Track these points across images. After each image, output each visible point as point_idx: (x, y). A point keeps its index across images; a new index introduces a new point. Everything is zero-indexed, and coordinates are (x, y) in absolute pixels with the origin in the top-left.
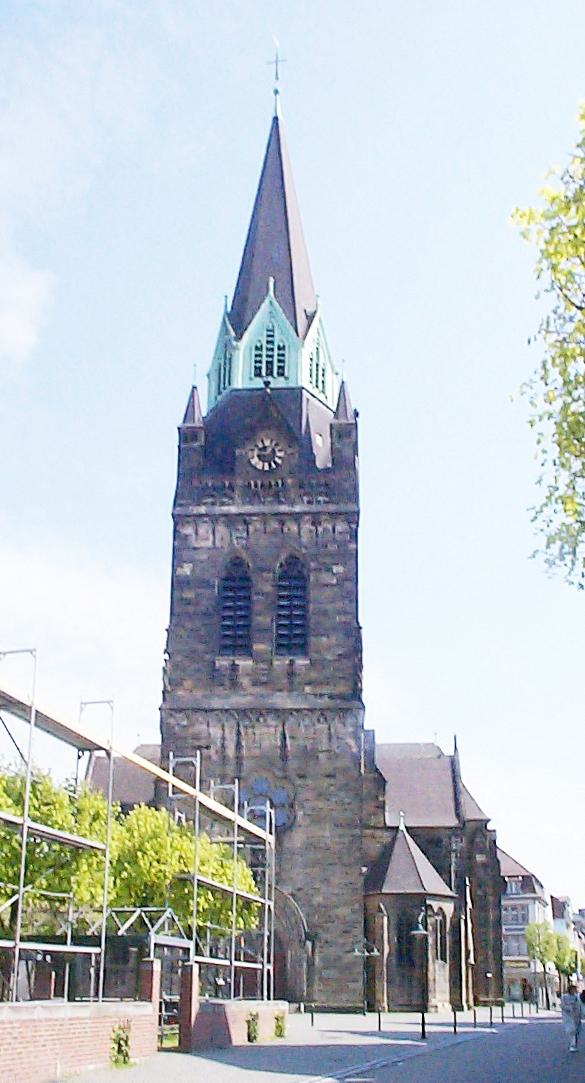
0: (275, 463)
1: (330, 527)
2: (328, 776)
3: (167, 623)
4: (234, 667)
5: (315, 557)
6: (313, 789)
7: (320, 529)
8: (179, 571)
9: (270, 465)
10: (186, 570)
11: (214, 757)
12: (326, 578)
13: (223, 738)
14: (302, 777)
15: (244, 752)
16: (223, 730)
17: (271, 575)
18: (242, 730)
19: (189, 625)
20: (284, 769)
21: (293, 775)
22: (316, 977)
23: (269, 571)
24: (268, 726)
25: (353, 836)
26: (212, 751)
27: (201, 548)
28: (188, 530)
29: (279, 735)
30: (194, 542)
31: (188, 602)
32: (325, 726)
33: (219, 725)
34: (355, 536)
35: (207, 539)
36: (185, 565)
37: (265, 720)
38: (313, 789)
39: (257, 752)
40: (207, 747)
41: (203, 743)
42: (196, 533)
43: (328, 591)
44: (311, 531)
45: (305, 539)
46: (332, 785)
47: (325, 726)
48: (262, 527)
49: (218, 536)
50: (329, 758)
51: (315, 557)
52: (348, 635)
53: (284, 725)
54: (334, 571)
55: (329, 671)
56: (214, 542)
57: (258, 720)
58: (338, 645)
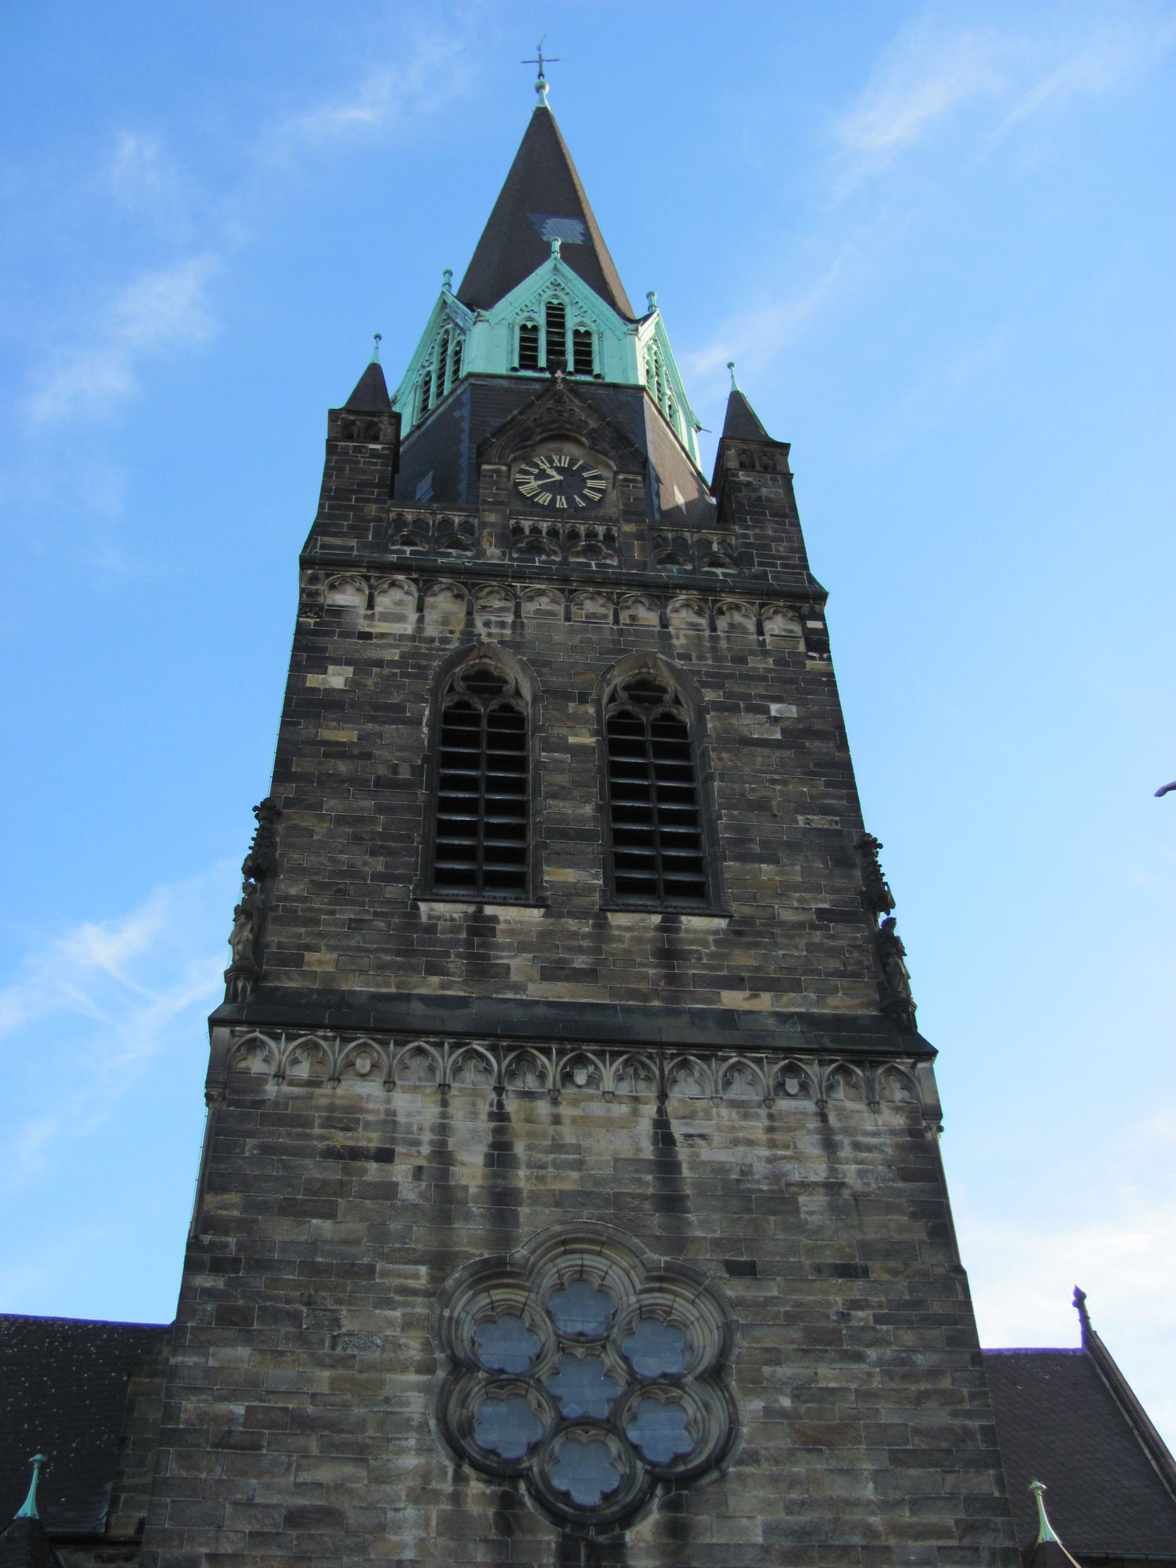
0: (585, 498)
1: (751, 625)
2: (847, 1271)
3: (262, 789)
4: (481, 927)
5: (717, 680)
6: (791, 1319)
7: (722, 623)
8: (313, 680)
9: (570, 500)
10: (336, 679)
12: (749, 724)
13: (443, 1129)
14: (744, 1270)
15: (522, 1178)
16: (444, 1103)
17: (591, 710)
18: (512, 1105)
19: (332, 805)
20: (678, 1243)
21: (708, 1261)
23: (583, 699)
24: (610, 1097)
25: (970, 1499)
26: (400, 1172)
27: (382, 636)
28: (348, 598)
29: (645, 1126)
30: (361, 621)
31: (339, 751)
32: (809, 1105)
33: (430, 1087)
34: (819, 643)
35: (402, 618)
36: (331, 669)
37: (592, 1080)
38: (791, 1319)
39: (570, 1181)
40: (385, 1156)
41: (371, 1139)
42: (371, 605)
43: (760, 757)
44: (694, 626)
45: (679, 643)
46: (855, 1305)
47: (809, 1105)
48: (560, 609)
49: (431, 616)
50: (834, 1208)
51: (717, 680)
52: (842, 862)
53: (663, 1096)
54: (773, 713)
55: (794, 951)
56: (420, 628)
57: (567, 1078)
58: (817, 888)
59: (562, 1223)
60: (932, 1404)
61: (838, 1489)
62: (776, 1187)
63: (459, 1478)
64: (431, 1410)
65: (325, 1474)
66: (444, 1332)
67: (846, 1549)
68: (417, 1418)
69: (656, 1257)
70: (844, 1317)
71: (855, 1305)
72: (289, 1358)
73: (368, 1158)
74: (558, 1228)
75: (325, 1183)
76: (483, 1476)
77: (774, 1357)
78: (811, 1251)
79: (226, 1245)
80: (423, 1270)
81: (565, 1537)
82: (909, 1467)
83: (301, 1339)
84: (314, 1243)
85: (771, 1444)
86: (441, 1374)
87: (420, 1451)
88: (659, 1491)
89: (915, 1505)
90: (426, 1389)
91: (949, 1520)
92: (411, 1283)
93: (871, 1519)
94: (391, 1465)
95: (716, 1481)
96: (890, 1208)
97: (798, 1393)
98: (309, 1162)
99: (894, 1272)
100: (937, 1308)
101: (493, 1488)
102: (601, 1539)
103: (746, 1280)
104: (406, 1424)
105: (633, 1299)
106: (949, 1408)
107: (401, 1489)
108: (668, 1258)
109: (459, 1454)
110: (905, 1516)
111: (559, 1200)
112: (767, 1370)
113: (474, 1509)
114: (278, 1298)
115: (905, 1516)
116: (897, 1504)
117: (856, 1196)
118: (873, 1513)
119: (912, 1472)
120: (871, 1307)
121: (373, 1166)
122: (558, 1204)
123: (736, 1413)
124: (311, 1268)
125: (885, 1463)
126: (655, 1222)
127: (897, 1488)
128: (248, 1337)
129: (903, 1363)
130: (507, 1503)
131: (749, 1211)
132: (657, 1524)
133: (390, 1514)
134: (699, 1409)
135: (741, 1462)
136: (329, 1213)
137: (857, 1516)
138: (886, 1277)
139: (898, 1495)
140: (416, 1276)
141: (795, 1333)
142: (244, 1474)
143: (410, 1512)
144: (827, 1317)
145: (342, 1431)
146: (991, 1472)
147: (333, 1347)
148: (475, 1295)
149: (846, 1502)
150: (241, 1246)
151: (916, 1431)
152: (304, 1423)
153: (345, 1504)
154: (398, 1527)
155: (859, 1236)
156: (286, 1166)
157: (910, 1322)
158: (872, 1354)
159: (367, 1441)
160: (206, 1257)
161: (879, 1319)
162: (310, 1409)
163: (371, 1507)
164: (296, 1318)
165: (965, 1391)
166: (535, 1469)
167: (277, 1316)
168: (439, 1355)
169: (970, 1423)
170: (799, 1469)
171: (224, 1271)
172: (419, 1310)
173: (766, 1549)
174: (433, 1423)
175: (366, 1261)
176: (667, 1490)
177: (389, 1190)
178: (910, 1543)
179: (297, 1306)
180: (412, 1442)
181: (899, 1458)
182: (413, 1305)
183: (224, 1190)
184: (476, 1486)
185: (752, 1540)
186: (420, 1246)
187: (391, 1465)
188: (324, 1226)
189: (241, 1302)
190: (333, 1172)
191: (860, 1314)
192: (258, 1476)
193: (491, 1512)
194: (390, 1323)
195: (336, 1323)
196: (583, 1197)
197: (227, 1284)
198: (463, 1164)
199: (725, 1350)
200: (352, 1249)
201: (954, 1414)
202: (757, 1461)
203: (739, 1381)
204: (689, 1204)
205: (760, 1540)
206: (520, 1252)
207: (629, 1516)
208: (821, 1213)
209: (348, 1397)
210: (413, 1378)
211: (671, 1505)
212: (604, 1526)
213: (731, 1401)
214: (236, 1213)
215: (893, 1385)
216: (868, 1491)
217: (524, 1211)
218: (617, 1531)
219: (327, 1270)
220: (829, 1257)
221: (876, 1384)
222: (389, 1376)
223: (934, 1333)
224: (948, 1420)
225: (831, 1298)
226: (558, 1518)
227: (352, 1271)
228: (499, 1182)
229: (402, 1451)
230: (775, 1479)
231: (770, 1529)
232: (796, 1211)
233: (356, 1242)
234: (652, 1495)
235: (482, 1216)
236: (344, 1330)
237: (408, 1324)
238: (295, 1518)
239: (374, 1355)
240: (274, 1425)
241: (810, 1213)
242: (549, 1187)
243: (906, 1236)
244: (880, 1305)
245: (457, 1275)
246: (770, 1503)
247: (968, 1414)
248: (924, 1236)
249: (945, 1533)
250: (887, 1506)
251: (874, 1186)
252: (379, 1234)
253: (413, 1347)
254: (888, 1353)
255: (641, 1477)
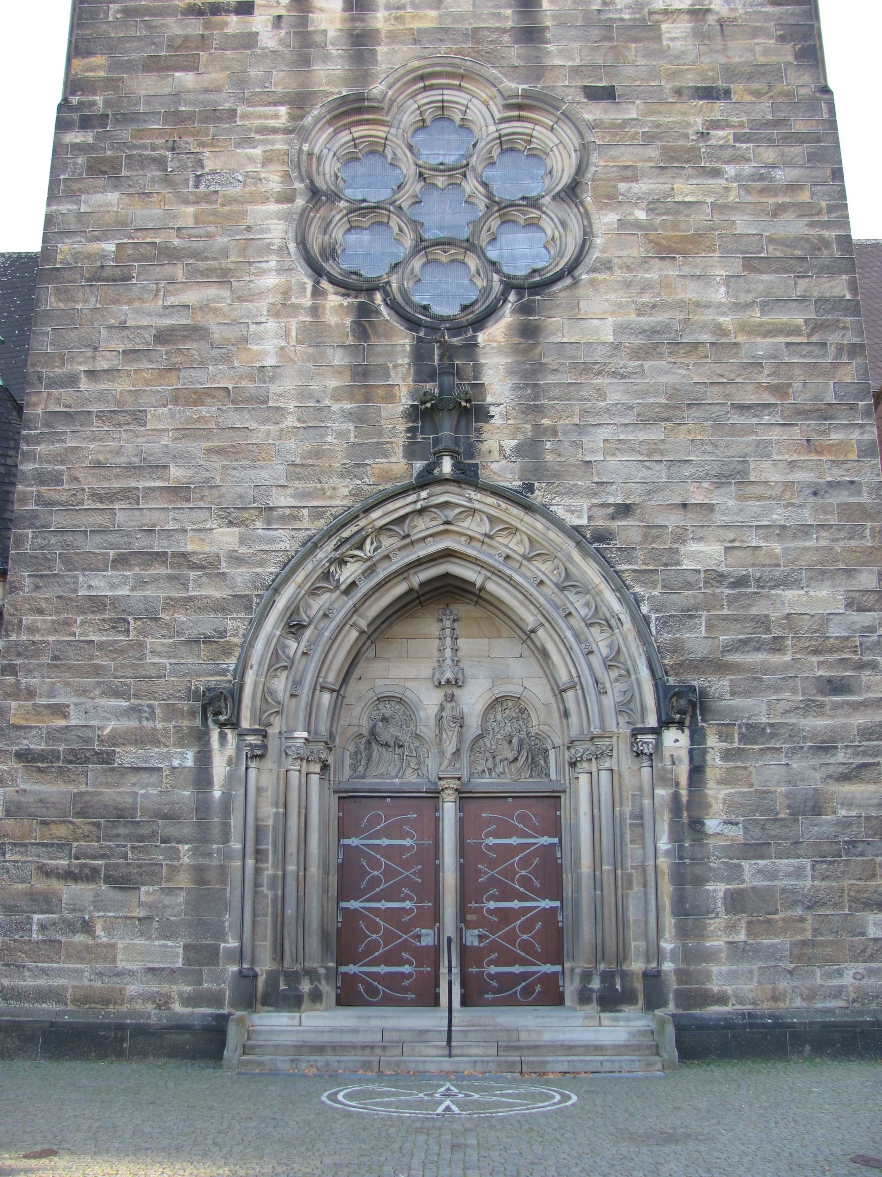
2: (708, 93)
6: (649, 139)
11: (269, 39)
20: (537, 71)
22: (718, 889)
25: (821, 302)
38: (649, 139)
46: (716, 125)
50: (700, 35)
59: (421, 58)
60: (789, 216)
61: (691, 292)
62: (638, 16)
63: (317, 292)
64: (291, 235)
65: (191, 296)
66: (303, 165)
67: (696, 345)
68: (277, 243)
69: (514, 86)
70: (703, 135)
71: (716, 125)
72: (155, 198)
73: (227, 12)
74: (416, 64)
75: (186, 38)
76: (343, 291)
77: (631, 174)
78: (673, 75)
79: (94, 103)
80: (283, 110)
81: (419, 340)
82: (762, 273)
83: (167, 181)
84: (178, 94)
85: (624, 253)
86: (300, 202)
87: (280, 271)
88: (512, 297)
89: (765, 306)
90: (285, 217)
91: (798, 320)
92: (272, 123)
93: (721, 319)
94: (253, 286)
95: (568, 287)
96: (756, 32)
97: (653, 206)
98: (170, 21)
99: (757, 94)
100: (799, 126)
101: (350, 300)
102: (455, 341)
103: (604, 104)
104: (267, 249)
105: (492, 128)
106: (806, 220)
107: (262, 305)
108: (526, 87)
109: (317, 271)
110: (756, 316)
111: (416, 37)
112: (623, 186)
113: (331, 319)
114: (144, 147)
115: (756, 316)
116: (750, 305)
117: (721, 23)
118: (723, 314)
119: (765, 277)
120: (733, 127)
121: (233, 19)
122: (415, 42)
123: (590, 225)
124: (176, 117)
125: (737, 267)
126: (514, 54)
127: (748, 291)
128: (116, 182)
129: (762, 178)
130: (364, 312)
131: (611, 39)
132: (509, 327)
133: (253, 328)
134: (556, 227)
135: (594, 270)
136: (192, 67)
137: (708, 316)
138: (748, 98)
139: (750, 298)
140: (276, 116)
141: (653, 152)
142: (116, 302)
143: (272, 325)
144: (686, 136)
145: (206, 258)
146: (845, 277)
147: (197, 187)
148: (336, 133)
149: (697, 304)
150: (108, 104)
151: (771, 240)
152: (170, 254)
153: (211, 322)
154: (260, 338)
155: (722, 60)
156: (149, 27)
157: (769, 140)
158: (730, 170)
159: (232, 266)
160: (76, 116)
161: (738, 138)
162: (176, 242)
163: (235, 322)
164: (161, 162)
165: (824, 204)
166: (394, 286)
167: (143, 163)
168: (298, 185)
169: (826, 234)
170: (653, 276)
171: (93, 127)
172: (279, 146)
173: (616, 347)
174: (292, 246)
175: (227, 106)
176: (520, 296)
177: (249, 40)
178: (759, 340)
179: (162, 152)
180: (273, 264)
181: (752, 264)
182: (273, 143)
183: (89, 54)
184: (334, 299)
185: (603, 339)
186: (279, 89)
187: (253, 286)
188: (187, 79)
189: (109, 153)
190: (195, 27)
191: (720, 133)
192: (130, 302)
193: (348, 321)
194: (251, 159)
195: (200, 163)
196: (442, 33)
197: (96, 138)
198: (322, 10)
199: (581, 170)
200: (213, 97)
201: (811, 225)
202: (610, 269)
203: (595, 197)
204: (548, 35)
205: (611, 339)
206: (377, 89)
207: (480, 322)
208: (684, 39)
209: (211, 229)
210: (273, 207)
211: (525, 309)
212: (457, 329)
213: (586, 215)
214: (102, 74)
215: (749, 199)
216: (720, 295)
217: (382, 50)
218: (470, 333)
219: (191, 116)
220: (690, 80)
221: (732, 198)
222: (249, 208)
223: (797, 151)
224: (806, 231)
225: (691, 119)
226: (412, 324)
227: (214, 116)
228: (358, 24)
229: (262, 272)
230: (628, 285)
231: (621, 329)
232: (659, 38)
233: (218, 90)
234: (505, 301)
235: (341, 57)
236: (207, 170)
237: (267, 160)
238: (163, 337)
239: (236, 190)
240: (143, 258)
241: (673, 39)
242: (408, 26)
243: (773, 59)
244: (741, 125)
245: (316, 112)
246: (621, 306)
247: (826, 225)
248: (790, 58)
249: (796, 331)
250: (738, 307)
251: (741, 11)
252: (240, 81)
253: (274, 181)
254: (747, 169)
255: (497, 287)
